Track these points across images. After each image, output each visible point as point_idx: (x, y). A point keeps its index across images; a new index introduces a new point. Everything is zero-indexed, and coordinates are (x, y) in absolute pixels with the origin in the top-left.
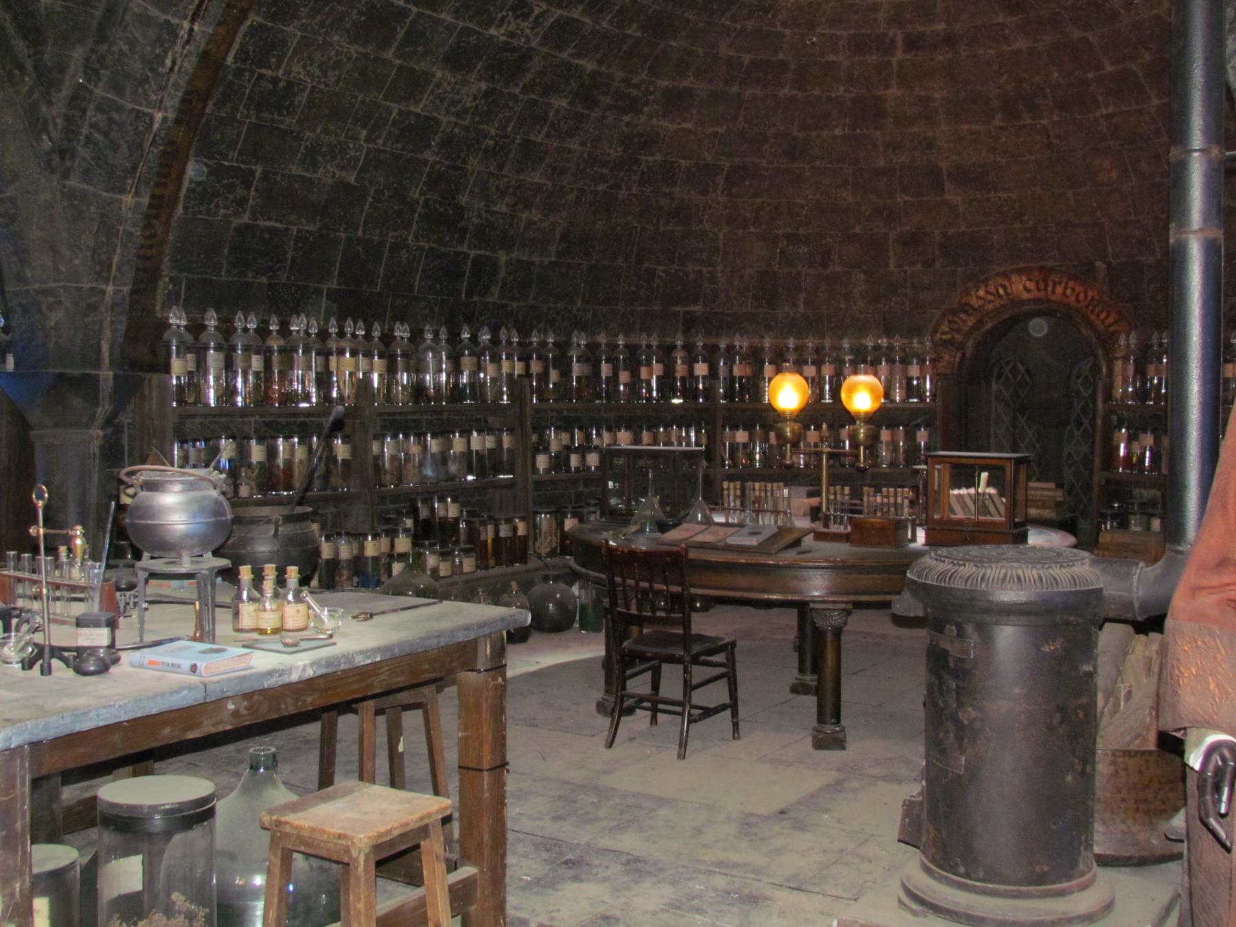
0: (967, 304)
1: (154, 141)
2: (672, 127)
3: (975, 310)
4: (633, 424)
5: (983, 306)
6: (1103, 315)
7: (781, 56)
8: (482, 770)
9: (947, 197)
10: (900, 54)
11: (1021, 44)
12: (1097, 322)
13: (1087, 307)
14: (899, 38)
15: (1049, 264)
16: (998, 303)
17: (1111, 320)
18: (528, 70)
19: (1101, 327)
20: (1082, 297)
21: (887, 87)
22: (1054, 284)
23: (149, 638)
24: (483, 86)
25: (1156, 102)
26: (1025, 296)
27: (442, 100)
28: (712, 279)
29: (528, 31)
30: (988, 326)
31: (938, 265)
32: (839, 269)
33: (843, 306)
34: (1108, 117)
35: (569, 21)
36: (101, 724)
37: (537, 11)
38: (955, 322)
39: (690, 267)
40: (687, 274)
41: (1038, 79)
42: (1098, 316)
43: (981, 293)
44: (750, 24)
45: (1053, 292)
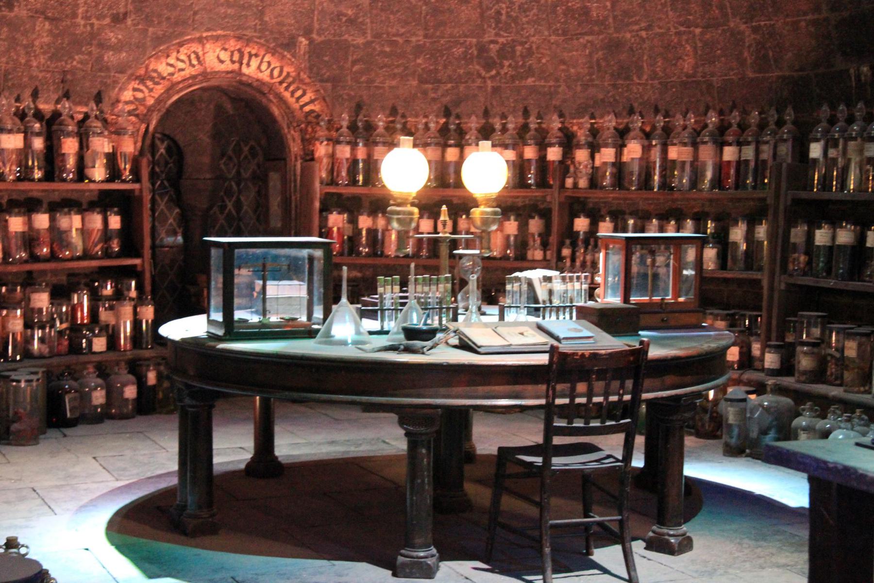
0: (155, 71)
3: (164, 78)
5: (172, 74)
6: (299, 93)
12: (292, 100)
13: (281, 83)
15: (249, 33)
16: (189, 72)
17: (306, 99)
19: (296, 106)
20: (276, 73)
22: (250, 56)
26: (222, 67)
31: (129, 22)
32: (24, 13)
33: (23, 61)
38: (141, 91)
42: (293, 93)
43: (172, 60)
45: (248, 65)
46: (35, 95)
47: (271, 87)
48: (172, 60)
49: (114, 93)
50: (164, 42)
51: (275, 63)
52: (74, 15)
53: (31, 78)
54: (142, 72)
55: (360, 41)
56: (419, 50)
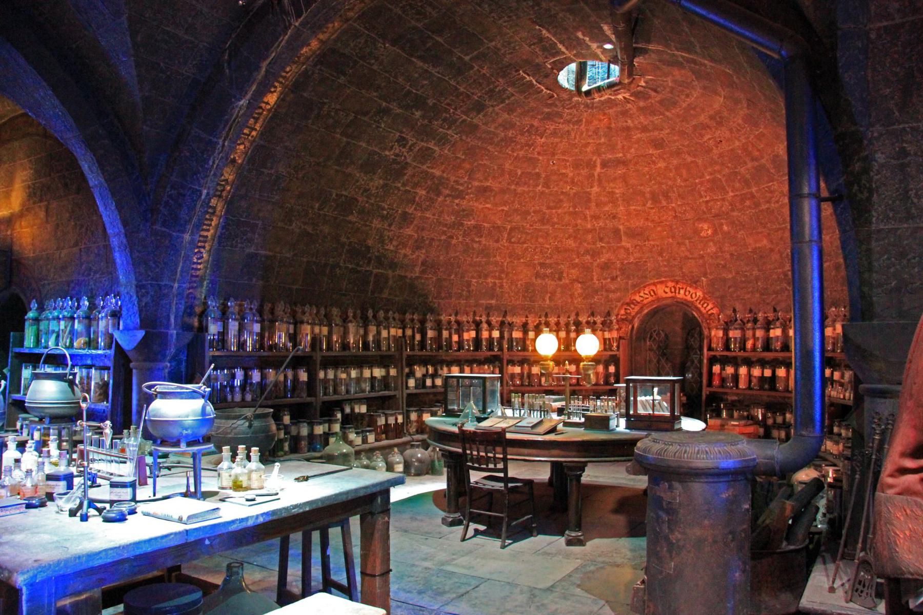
1: (202, 205)
2: (481, 206)
4: (460, 363)
7: (537, 170)
8: (374, 576)
9: (623, 244)
10: (598, 169)
11: (661, 164)
12: (702, 309)
14: (599, 162)
16: (650, 299)
17: (709, 307)
18: (405, 174)
19: (704, 311)
21: (592, 187)
23: (158, 496)
24: (381, 182)
25: (731, 194)
26: (664, 295)
27: (360, 189)
28: (501, 286)
29: (405, 154)
30: (646, 311)
32: (567, 281)
34: (707, 202)
35: (428, 149)
36: (109, 560)
37: (410, 143)
39: (489, 280)
40: (487, 283)
41: (670, 183)
43: (642, 294)
44: (521, 153)
46: (577, 315)
47: (692, 303)
48: (642, 294)
49: (616, 311)
50: (637, 288)
51: (692, 291)
52: (592, 279)
53: (575, 307)
54: (628, 301)
55: (730, 276)
56: (757, 279)
